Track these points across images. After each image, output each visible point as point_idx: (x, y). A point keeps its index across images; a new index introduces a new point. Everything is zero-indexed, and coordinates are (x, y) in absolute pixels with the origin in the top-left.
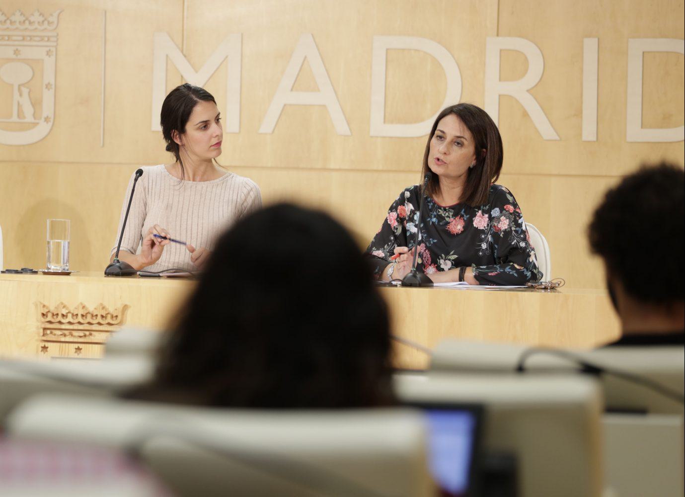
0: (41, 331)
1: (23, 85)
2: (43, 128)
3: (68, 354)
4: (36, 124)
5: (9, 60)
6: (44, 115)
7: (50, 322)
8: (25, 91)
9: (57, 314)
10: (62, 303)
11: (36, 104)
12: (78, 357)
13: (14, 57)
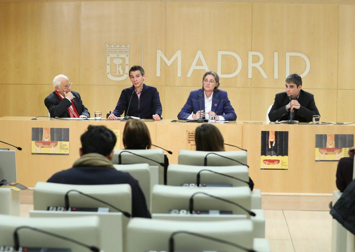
5: (115, 58)
7: (191, 136)
9: (193, 134)
11: (124, 69)
13: (117, 57)
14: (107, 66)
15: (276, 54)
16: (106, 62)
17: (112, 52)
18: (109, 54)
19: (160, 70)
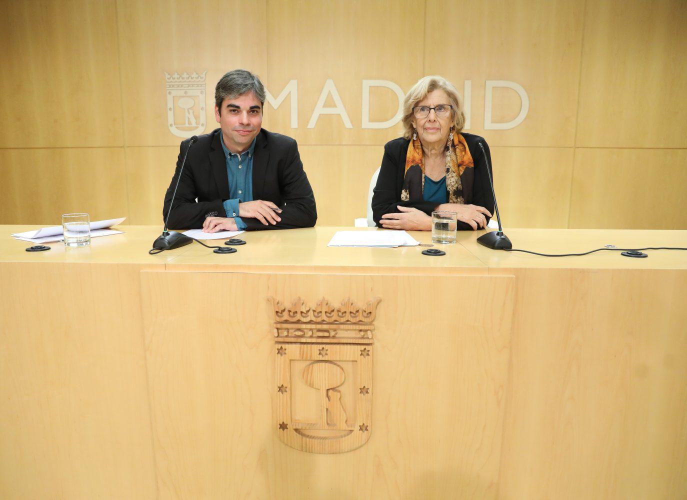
0: (276, 330)
1: (190, 109)
3: (311, 356)
5: (183, 97)
6: (201, 123)
7: (286, 322)
8: (191, 111)
10: (300, 298)
11: (197, 117)
12: (323, 359)
14: (169, 111)
15: (468, 84)
16: (166, 105)
17: (175, 86)
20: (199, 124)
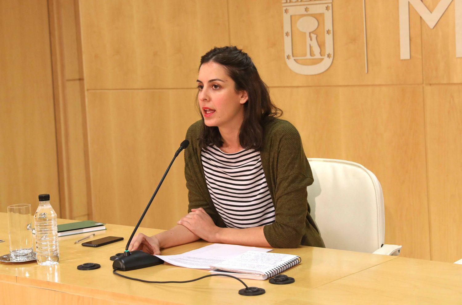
1: (313, 32)
2: (327, 62)
4: (322, 59)
6: (327, 53)
11: (321, 45)
13: (305, 13)
14: (285, 37)
16: (282, 27)
18: (288, 8)
19: (410, 40)
20: (324, 56)
